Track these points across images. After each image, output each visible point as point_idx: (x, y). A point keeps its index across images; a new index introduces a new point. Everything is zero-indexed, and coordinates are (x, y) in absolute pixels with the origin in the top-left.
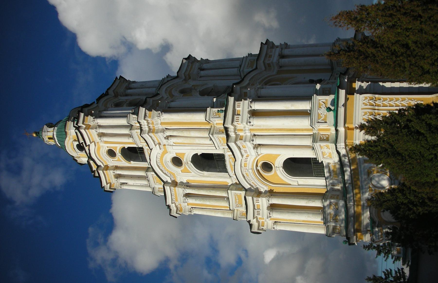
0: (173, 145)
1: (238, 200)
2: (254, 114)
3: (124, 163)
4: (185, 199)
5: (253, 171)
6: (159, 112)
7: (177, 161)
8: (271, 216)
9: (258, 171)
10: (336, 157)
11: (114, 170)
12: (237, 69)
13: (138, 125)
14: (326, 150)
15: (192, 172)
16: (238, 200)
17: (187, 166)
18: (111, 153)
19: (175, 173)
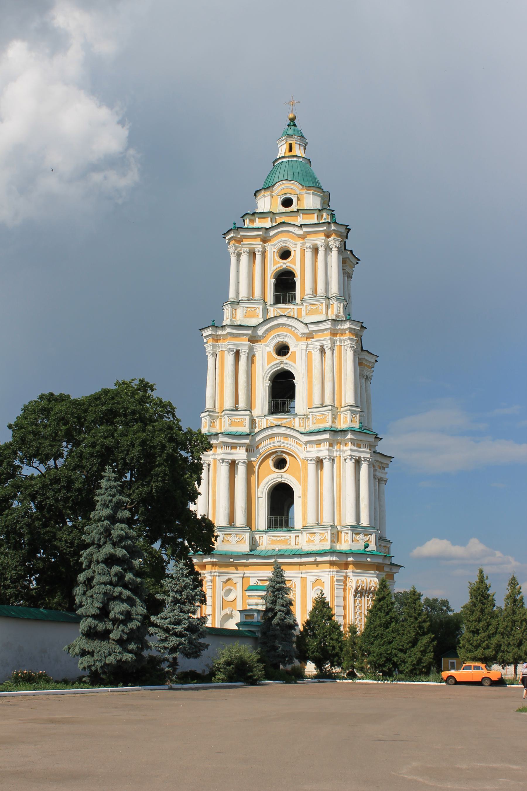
1: (236, 421)
4: (233, 351)
5: (277, 447)
8: (224, 463)
14: (318, 537)
16: (236, 421)
18: (285, 254)
19: (266, 344)
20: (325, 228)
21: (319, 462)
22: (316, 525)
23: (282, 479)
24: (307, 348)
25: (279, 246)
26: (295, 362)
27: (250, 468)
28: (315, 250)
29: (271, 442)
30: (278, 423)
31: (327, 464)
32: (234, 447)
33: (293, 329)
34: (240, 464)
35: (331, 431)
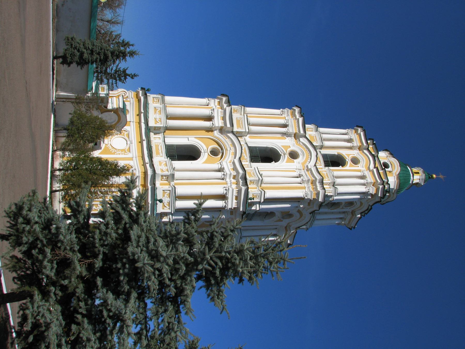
0: (296, 169)
2: (223, 197)
3: (344, 153)
6: (306, 198)
7: (293, 155)
8: (211, 111)
9: (222, 149)
10: (156, 162)
11: (353, 146)
12: (244, 235)
13: (325, 186)
14: (165, 168)
15: (281, 147)
16: (240, 123)
17: (285, 152)
18: (355, 161)
20: (379, 181)
21: (220, 170)
22: (174, 168)
23: (203, 153)
24: (298, 169)
25: (359, 157)
26: (287, 162)
27: (209, 130)
28: (363, 177)
29: (230, 145)
30: (243, 148)
31: (219, 174)
32: (224, 118)
33: (309, 161)
34: (211, 122)
35: (246, 175)
